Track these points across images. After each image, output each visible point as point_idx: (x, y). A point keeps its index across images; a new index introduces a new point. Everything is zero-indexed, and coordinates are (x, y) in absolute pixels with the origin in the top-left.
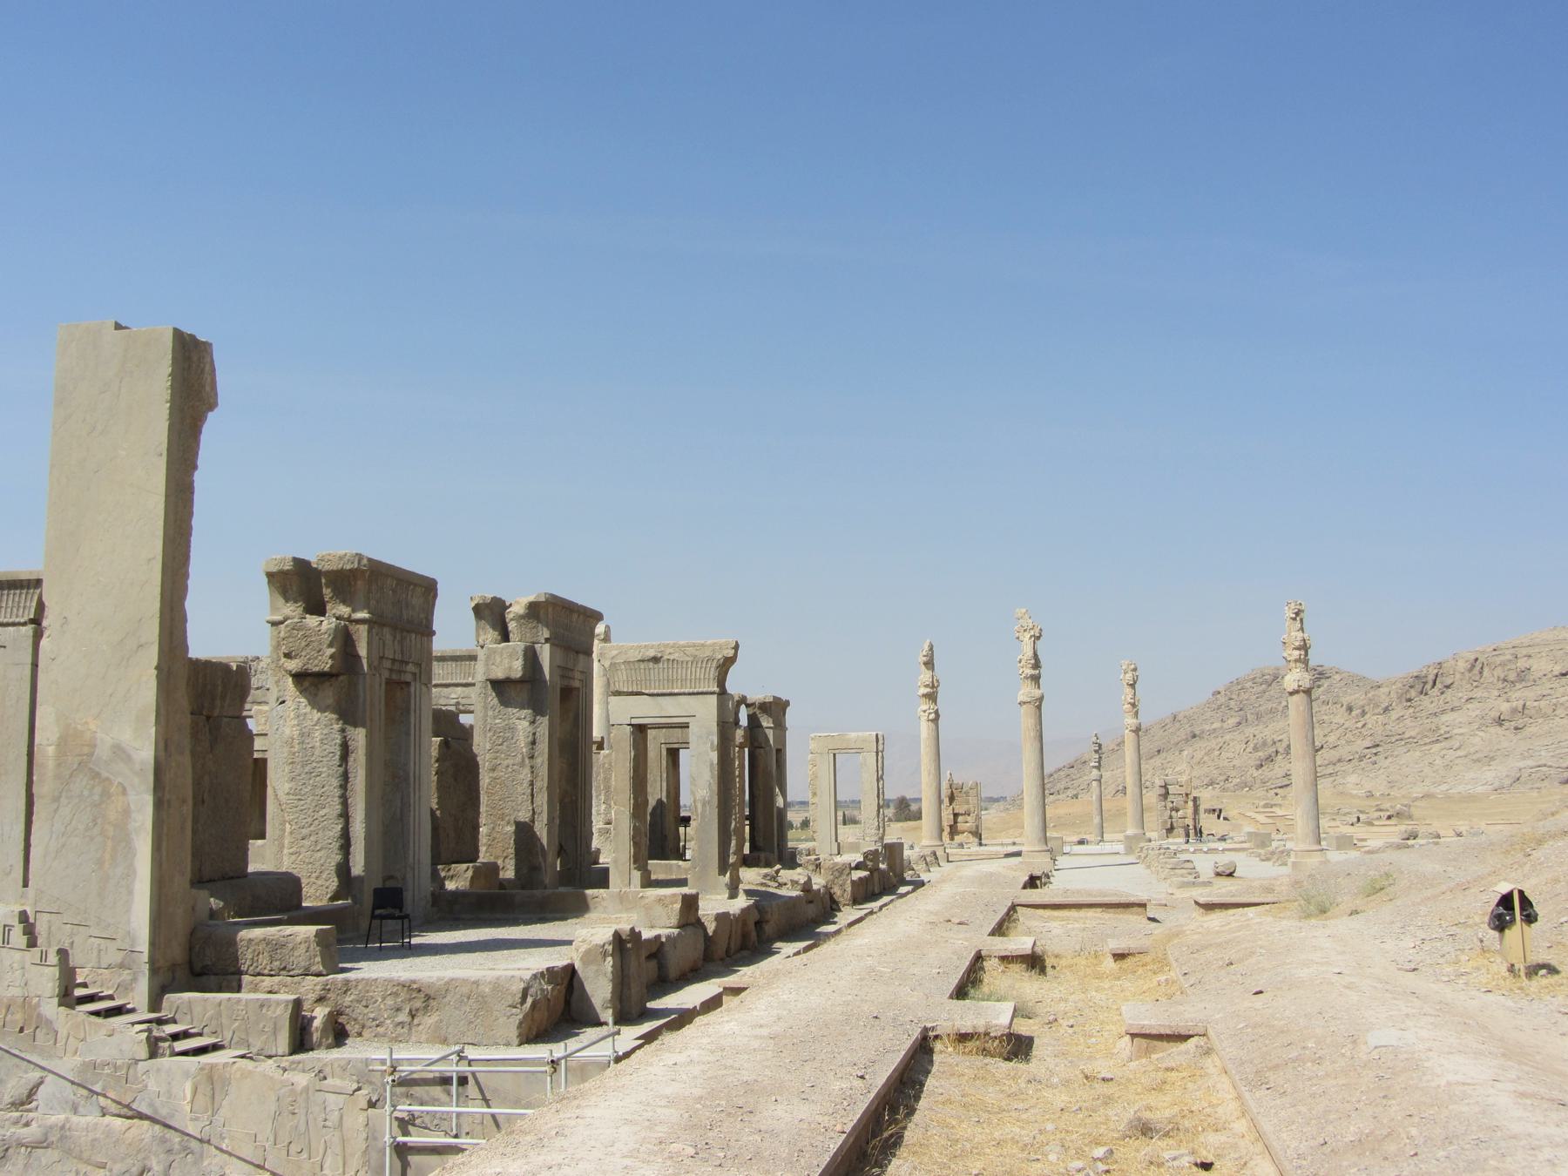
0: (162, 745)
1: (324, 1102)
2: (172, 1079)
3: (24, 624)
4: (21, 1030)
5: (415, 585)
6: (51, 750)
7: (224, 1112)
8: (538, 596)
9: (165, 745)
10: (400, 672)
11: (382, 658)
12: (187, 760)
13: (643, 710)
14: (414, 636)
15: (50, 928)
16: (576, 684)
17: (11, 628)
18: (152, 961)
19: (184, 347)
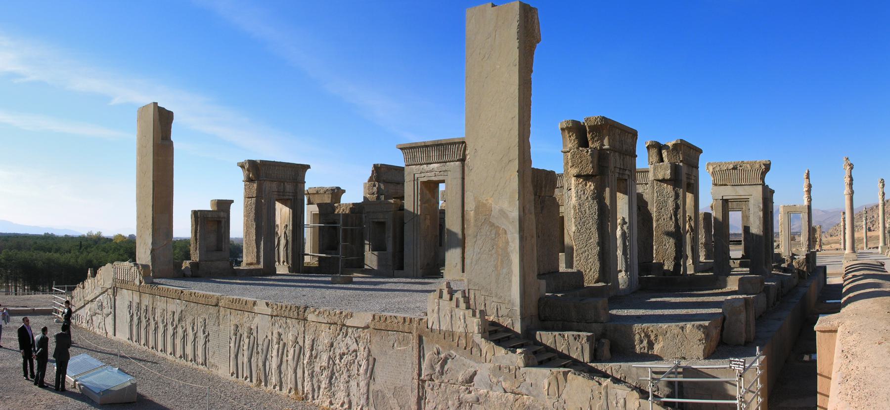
0: (522, 209)
1: (616, 395)
2: (537, 378)
3: (456, 161)
4: (465, 349)
5: (629, 133)
6: (472, 213)
7: (564, 396)
8: (677, 141)
9: (523, 210)
10: (623, 174)
11: (615, 167)
12: (533, 217)
13: (728, 192)
14: (628, 157)
15: (475, 296)
16: (692, 182)
17: (452, 163)
18: (521, 314)
19: (525, 11)
